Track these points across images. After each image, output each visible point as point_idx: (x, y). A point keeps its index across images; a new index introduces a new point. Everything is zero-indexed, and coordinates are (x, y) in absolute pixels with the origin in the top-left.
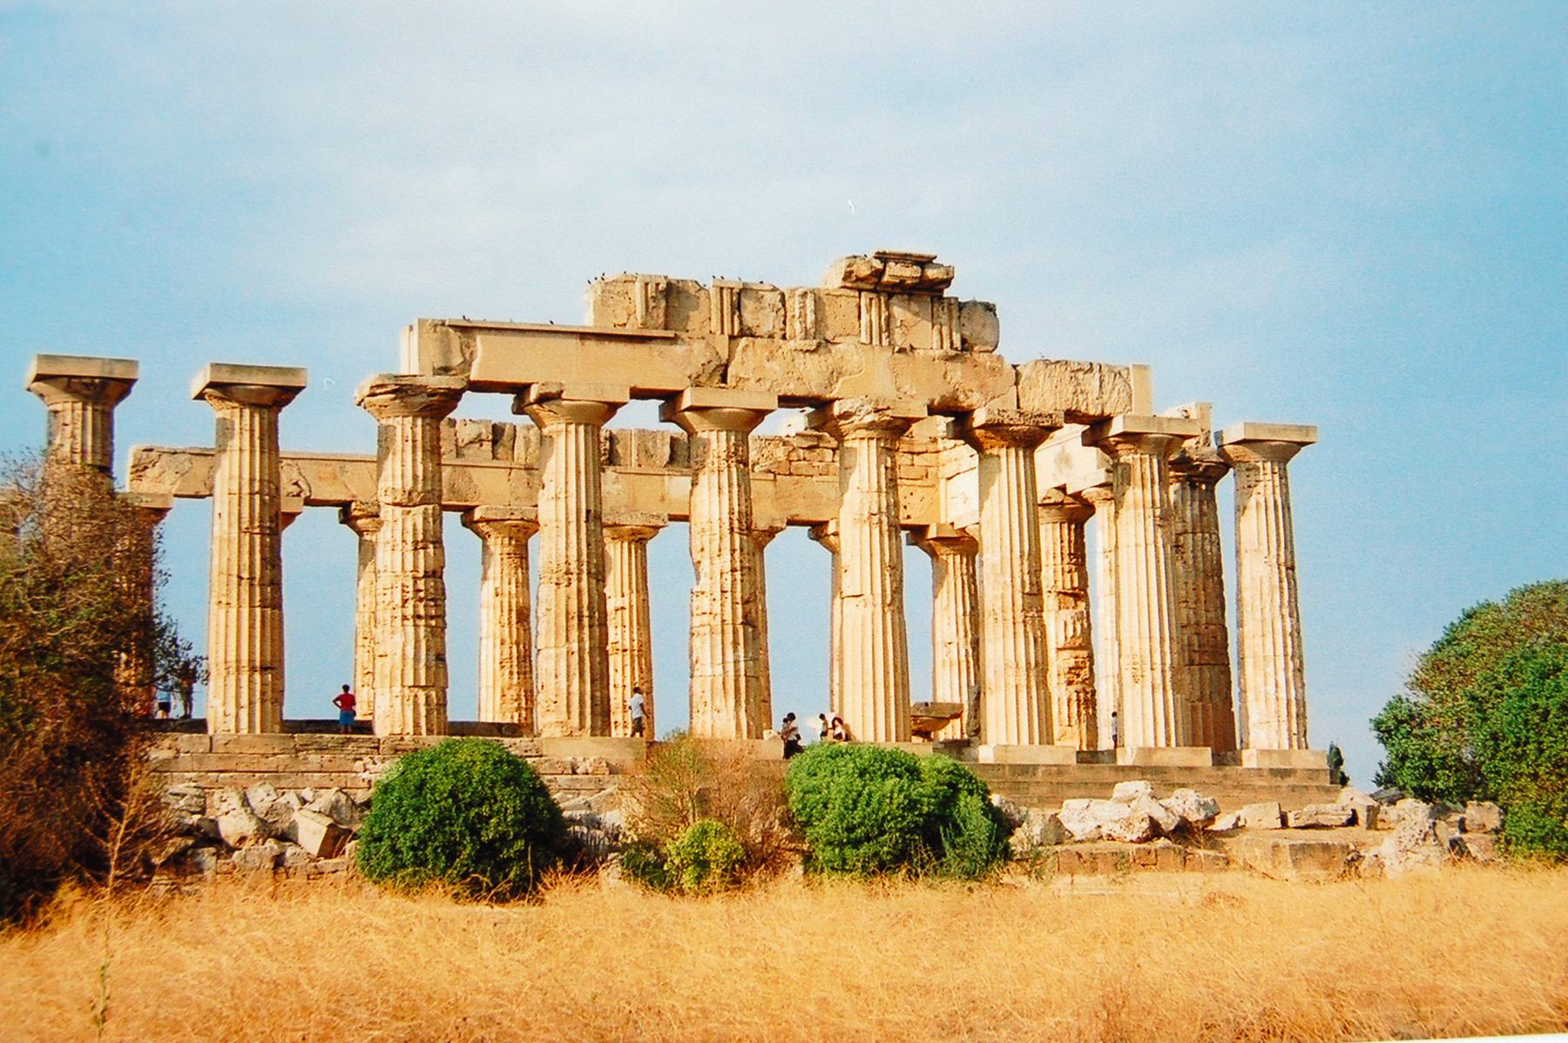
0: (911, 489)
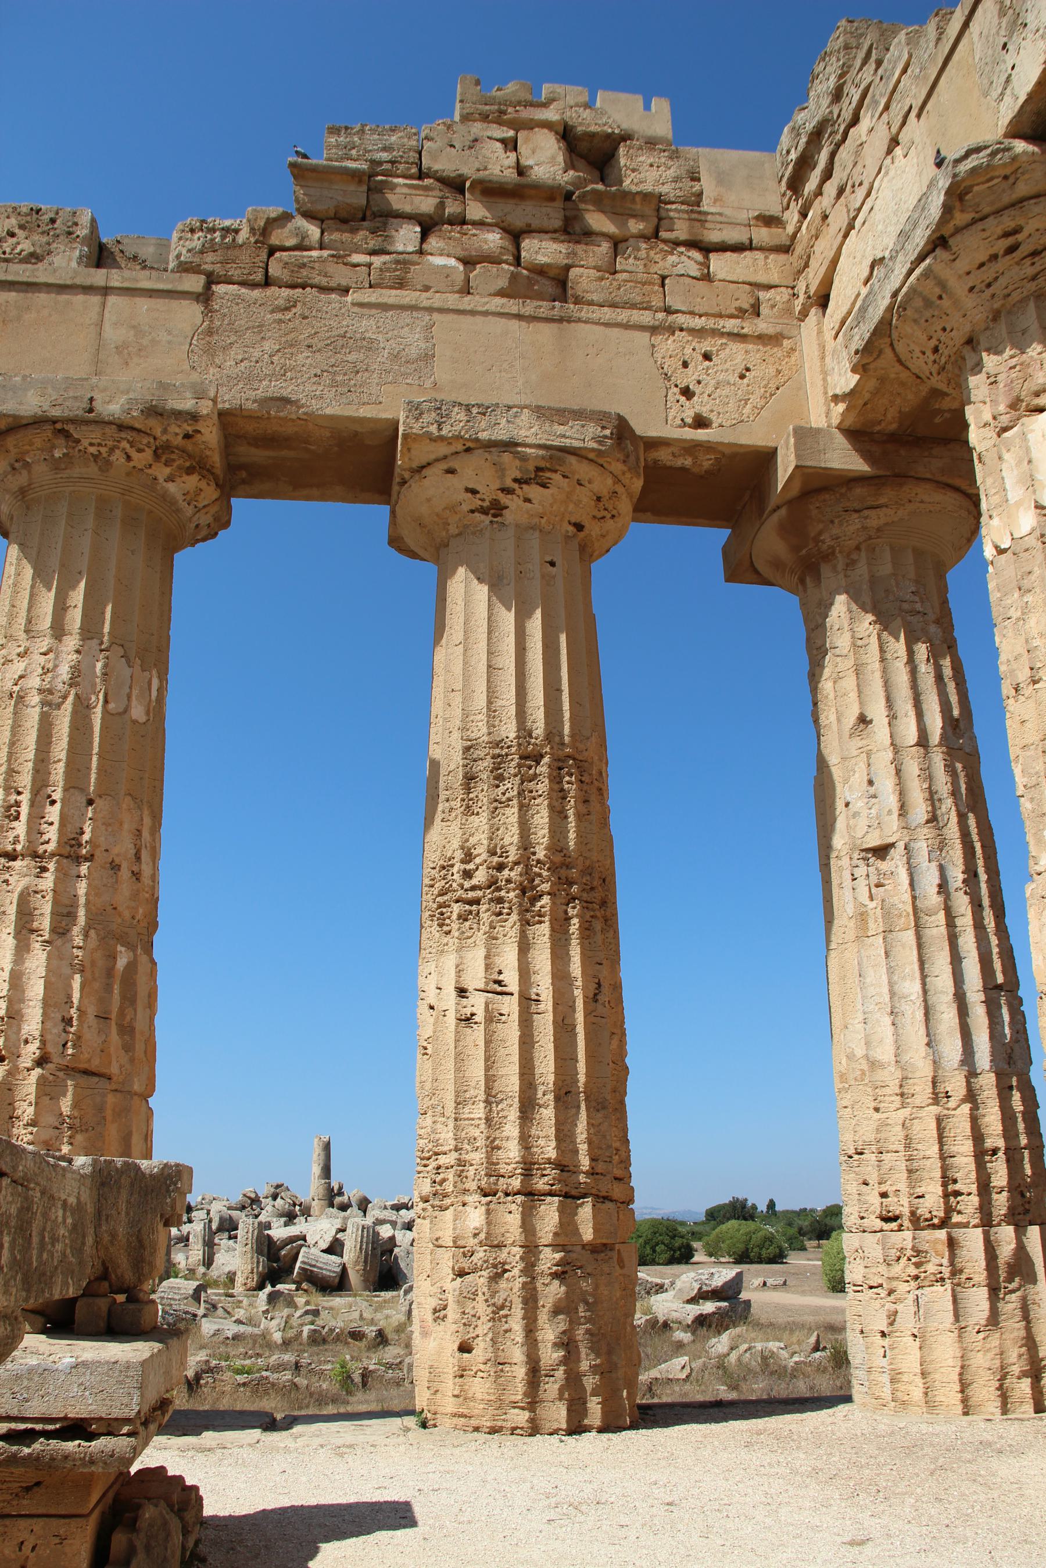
0: (707, 345)
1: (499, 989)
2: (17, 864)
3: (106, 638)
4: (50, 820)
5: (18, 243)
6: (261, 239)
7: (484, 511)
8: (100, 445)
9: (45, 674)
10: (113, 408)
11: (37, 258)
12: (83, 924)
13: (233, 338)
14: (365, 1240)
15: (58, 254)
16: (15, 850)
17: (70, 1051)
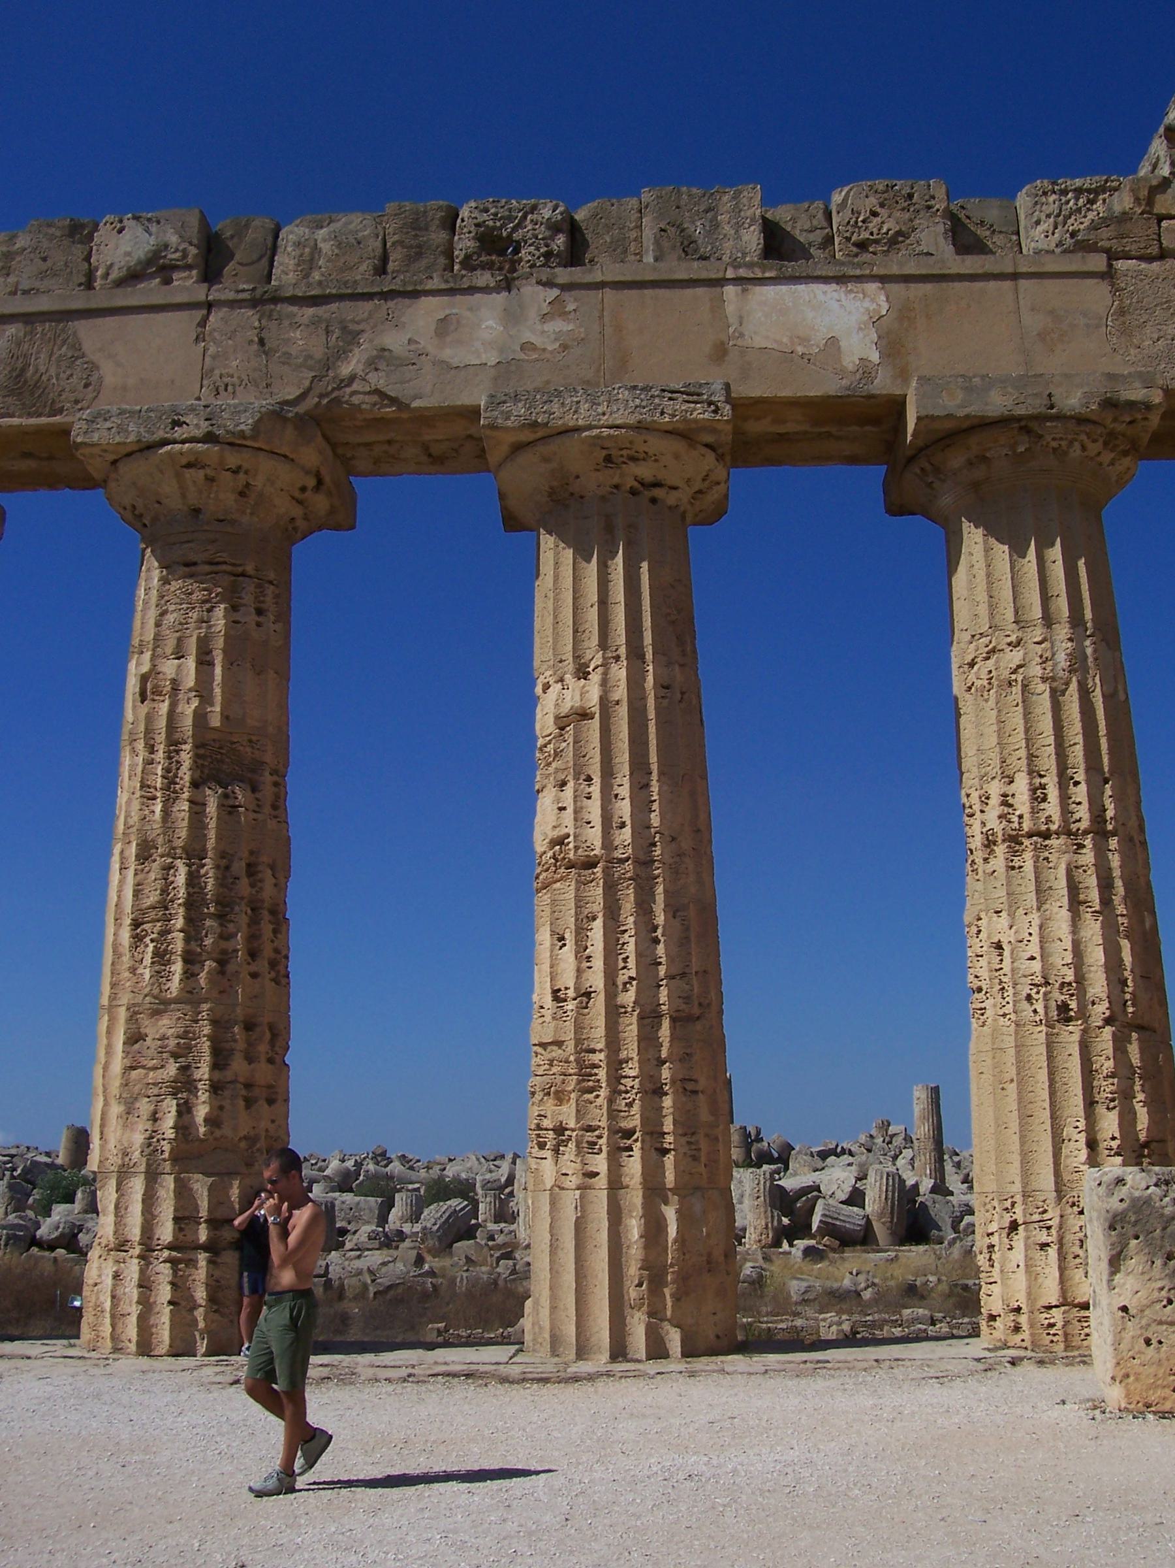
2: (1054, 842)
3: (1089, 625)
4: (1078, 800)
5: (883, 223)
6: (1148, 208)
8: (1061, 439)
9: (1044, 662)
10: (1072, 401)
11: (904, 236)
12: (1123, 893)
13: (1145, 317)
14: (890, 1188)
15: (923, 230)
16: (1048, 829)
17: (1130, 1010)
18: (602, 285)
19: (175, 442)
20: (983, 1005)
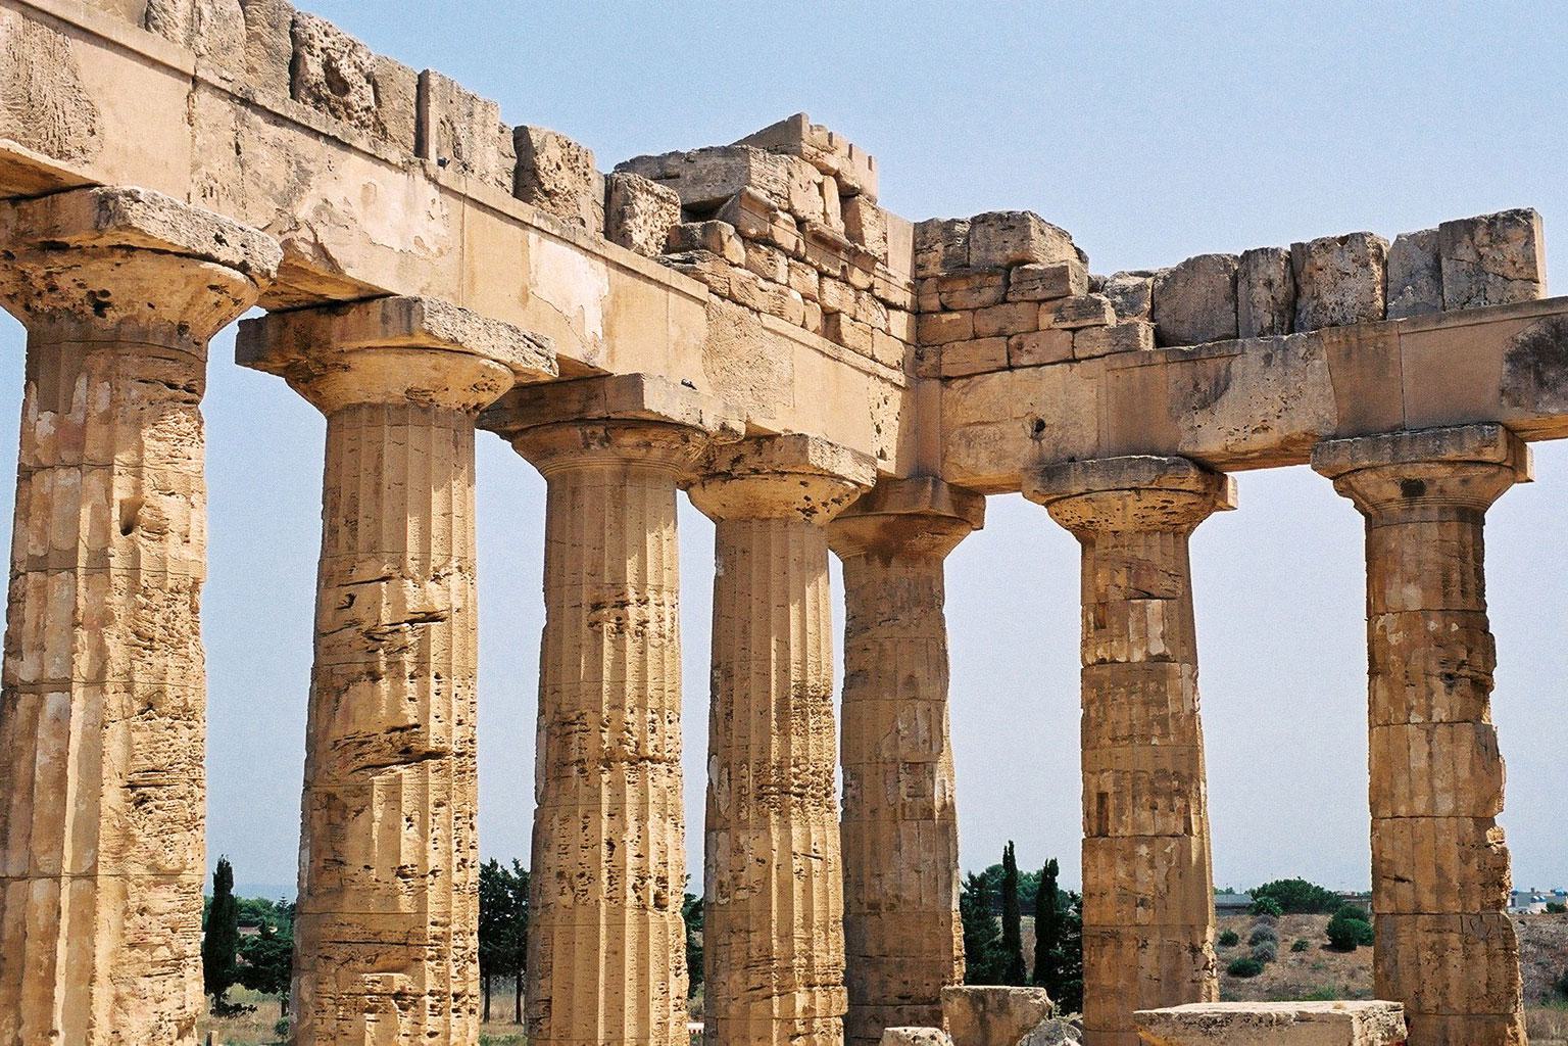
1: (816, 855)
7: (804, 511)
18: (464, 197)
19: (217, 261)
20: (585, 888)
